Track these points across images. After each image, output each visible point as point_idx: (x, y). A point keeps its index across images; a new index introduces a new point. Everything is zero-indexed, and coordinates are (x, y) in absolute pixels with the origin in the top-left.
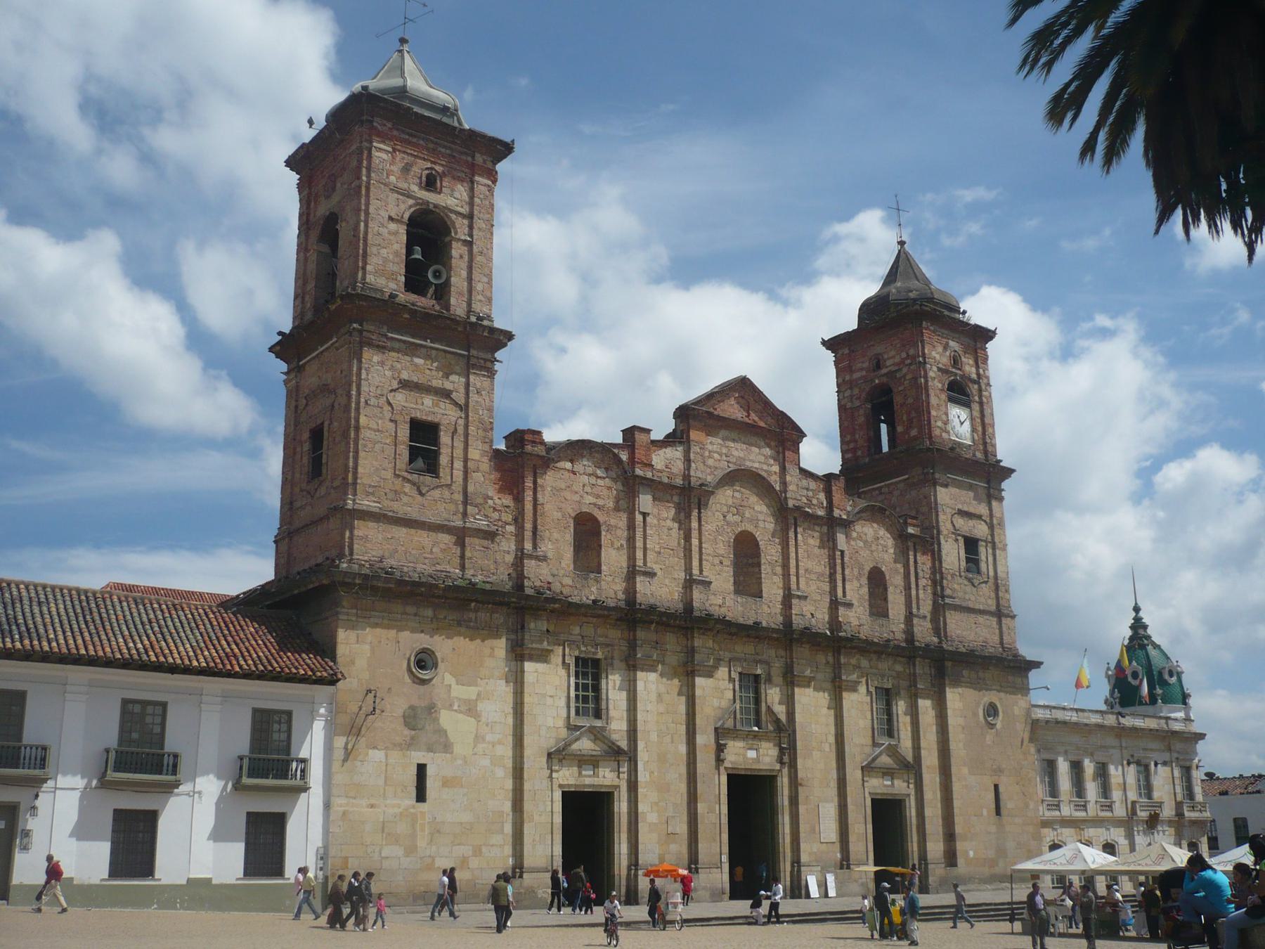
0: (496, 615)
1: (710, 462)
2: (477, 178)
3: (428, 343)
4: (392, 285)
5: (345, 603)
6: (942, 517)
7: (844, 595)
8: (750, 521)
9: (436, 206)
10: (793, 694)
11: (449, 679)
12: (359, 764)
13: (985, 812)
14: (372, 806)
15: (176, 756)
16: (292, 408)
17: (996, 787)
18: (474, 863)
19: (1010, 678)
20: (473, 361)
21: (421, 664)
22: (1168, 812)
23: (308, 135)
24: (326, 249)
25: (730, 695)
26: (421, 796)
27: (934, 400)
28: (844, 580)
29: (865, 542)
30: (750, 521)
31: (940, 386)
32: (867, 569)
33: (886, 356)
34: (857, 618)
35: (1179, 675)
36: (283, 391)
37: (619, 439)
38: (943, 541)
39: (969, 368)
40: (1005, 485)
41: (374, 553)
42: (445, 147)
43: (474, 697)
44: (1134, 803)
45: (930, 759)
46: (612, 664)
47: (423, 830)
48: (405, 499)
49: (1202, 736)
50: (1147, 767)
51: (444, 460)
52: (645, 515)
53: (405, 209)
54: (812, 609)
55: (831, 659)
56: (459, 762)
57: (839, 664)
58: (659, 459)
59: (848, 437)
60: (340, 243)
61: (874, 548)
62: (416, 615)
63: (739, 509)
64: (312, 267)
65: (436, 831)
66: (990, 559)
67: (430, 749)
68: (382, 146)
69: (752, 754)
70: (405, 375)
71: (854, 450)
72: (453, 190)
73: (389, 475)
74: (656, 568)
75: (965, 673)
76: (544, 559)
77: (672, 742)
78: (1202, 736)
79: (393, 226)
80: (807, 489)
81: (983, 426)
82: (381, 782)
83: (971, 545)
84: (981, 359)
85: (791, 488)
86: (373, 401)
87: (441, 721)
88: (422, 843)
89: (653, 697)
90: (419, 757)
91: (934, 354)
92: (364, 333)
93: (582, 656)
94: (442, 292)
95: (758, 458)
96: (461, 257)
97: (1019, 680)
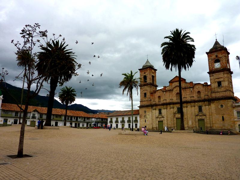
13: (220, 120)
17: (223, 117)
32: (197, 91)
74: (167, 99)
75: (215, 101)
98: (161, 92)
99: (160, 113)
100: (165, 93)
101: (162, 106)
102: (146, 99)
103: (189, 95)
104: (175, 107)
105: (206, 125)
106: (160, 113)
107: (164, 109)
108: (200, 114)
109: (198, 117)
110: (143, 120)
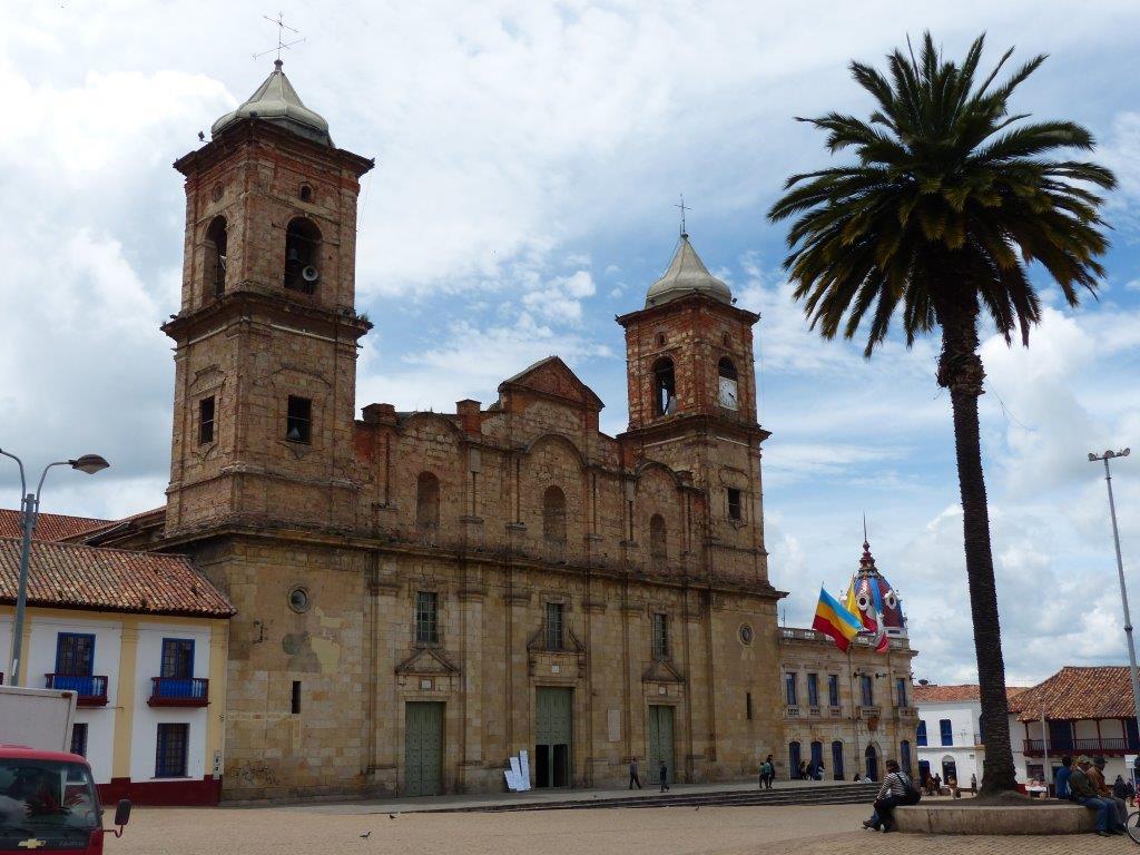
0: (356, 559)
1: (528, 429)
2: (344, 190)
3: (304, 332)
4: (275, 283)
5: (237, 551)
6: (712, 473)
7: (632, 540)
8: (558, 478)
9: (310, 215)
10: (589, 621)
11: (318, 611)
12: (246, 682)
13: (739, 715)
14: (258, 717)
15: (105, 679)
16: (183, 380)
17: (748, 695)
18: (338, 762)
19: (762, 606)
20: (340, 347)
21: (295, 600)
22: (886, 713)
23: (197, 146)
24: (212, 244)
25: (539, 621)
26: (296, 709)
27: (708, 375)
28: (632, 525)
29: (650, 494)
30: (558, 478)
31: (713, 362)
32: (650, 515)
33: (669, 335)
34: (640, 556)
35: (898, 602)
36: (173, 365)
37: (453, 410)
38: (712, 494)
39: (739, 348)
40: (762, 445)
41: (260, 509)
42: (318, 164)
43: (338, 626)
44: (859, 708)
45: (696, 674)
46: (447, 599)
47: (297, 736)
48: (285, 463)
49: (915, 653)
50: (869, 679)
51: (315, 430)
52: (474, 473)
53: (285, 216)
54: (606, 550)
55: (619, 592)
56: (326, 679)
57: (626, 594)
58: (486, 428)
59: (636, 400)
60: (229, 244)
61: (656, 497)
62: (293, 560)
63: (550, 467)
64: (200, 258)
65: (308, 735)
66: (750, 507)
67: (304, 669)
68: (268, 164)
69: (555, 669)
70: (285, 360)
71: (641, 411)
72: (324, 201)
73: (272, 443)
74: (483, 517)
76: (395, 511)
77: (493, 660)
78: (915, 653)
79: (275, 233)
80: (604, 450)
81: (747, 396)
82: (265, 697)
83: (734, 495)
84: (747, 339)
85: (592, 449)
86: (259, 382)
87: (313, 647)
88: (296, 746)
89: (479, 624)
90: (294, 676)
91: (709, 335)
92: (252, 325)
93: (424, 590)
94: (310, 288)
95: (566, 421)
96: (330, 258)
97: (768, 607)
98: (447, 448)
99: (428, 631)
100: (475, 456)
101: (450, 574)
102: (310, 467)
103: (613, 523)
104: (535, 598)
105: (683, 747)
106: (428, 631)
107: (463, 595)
108: (661, 671)
109: (655, 691)
110: (267, 683)
